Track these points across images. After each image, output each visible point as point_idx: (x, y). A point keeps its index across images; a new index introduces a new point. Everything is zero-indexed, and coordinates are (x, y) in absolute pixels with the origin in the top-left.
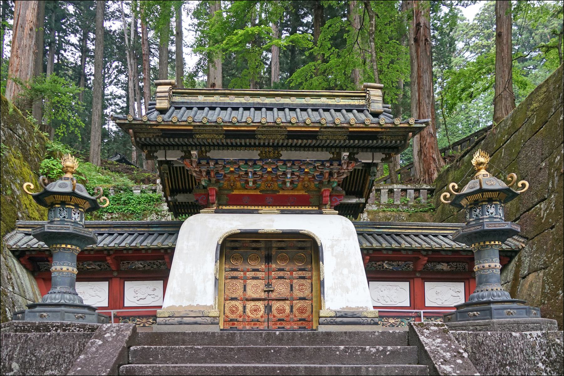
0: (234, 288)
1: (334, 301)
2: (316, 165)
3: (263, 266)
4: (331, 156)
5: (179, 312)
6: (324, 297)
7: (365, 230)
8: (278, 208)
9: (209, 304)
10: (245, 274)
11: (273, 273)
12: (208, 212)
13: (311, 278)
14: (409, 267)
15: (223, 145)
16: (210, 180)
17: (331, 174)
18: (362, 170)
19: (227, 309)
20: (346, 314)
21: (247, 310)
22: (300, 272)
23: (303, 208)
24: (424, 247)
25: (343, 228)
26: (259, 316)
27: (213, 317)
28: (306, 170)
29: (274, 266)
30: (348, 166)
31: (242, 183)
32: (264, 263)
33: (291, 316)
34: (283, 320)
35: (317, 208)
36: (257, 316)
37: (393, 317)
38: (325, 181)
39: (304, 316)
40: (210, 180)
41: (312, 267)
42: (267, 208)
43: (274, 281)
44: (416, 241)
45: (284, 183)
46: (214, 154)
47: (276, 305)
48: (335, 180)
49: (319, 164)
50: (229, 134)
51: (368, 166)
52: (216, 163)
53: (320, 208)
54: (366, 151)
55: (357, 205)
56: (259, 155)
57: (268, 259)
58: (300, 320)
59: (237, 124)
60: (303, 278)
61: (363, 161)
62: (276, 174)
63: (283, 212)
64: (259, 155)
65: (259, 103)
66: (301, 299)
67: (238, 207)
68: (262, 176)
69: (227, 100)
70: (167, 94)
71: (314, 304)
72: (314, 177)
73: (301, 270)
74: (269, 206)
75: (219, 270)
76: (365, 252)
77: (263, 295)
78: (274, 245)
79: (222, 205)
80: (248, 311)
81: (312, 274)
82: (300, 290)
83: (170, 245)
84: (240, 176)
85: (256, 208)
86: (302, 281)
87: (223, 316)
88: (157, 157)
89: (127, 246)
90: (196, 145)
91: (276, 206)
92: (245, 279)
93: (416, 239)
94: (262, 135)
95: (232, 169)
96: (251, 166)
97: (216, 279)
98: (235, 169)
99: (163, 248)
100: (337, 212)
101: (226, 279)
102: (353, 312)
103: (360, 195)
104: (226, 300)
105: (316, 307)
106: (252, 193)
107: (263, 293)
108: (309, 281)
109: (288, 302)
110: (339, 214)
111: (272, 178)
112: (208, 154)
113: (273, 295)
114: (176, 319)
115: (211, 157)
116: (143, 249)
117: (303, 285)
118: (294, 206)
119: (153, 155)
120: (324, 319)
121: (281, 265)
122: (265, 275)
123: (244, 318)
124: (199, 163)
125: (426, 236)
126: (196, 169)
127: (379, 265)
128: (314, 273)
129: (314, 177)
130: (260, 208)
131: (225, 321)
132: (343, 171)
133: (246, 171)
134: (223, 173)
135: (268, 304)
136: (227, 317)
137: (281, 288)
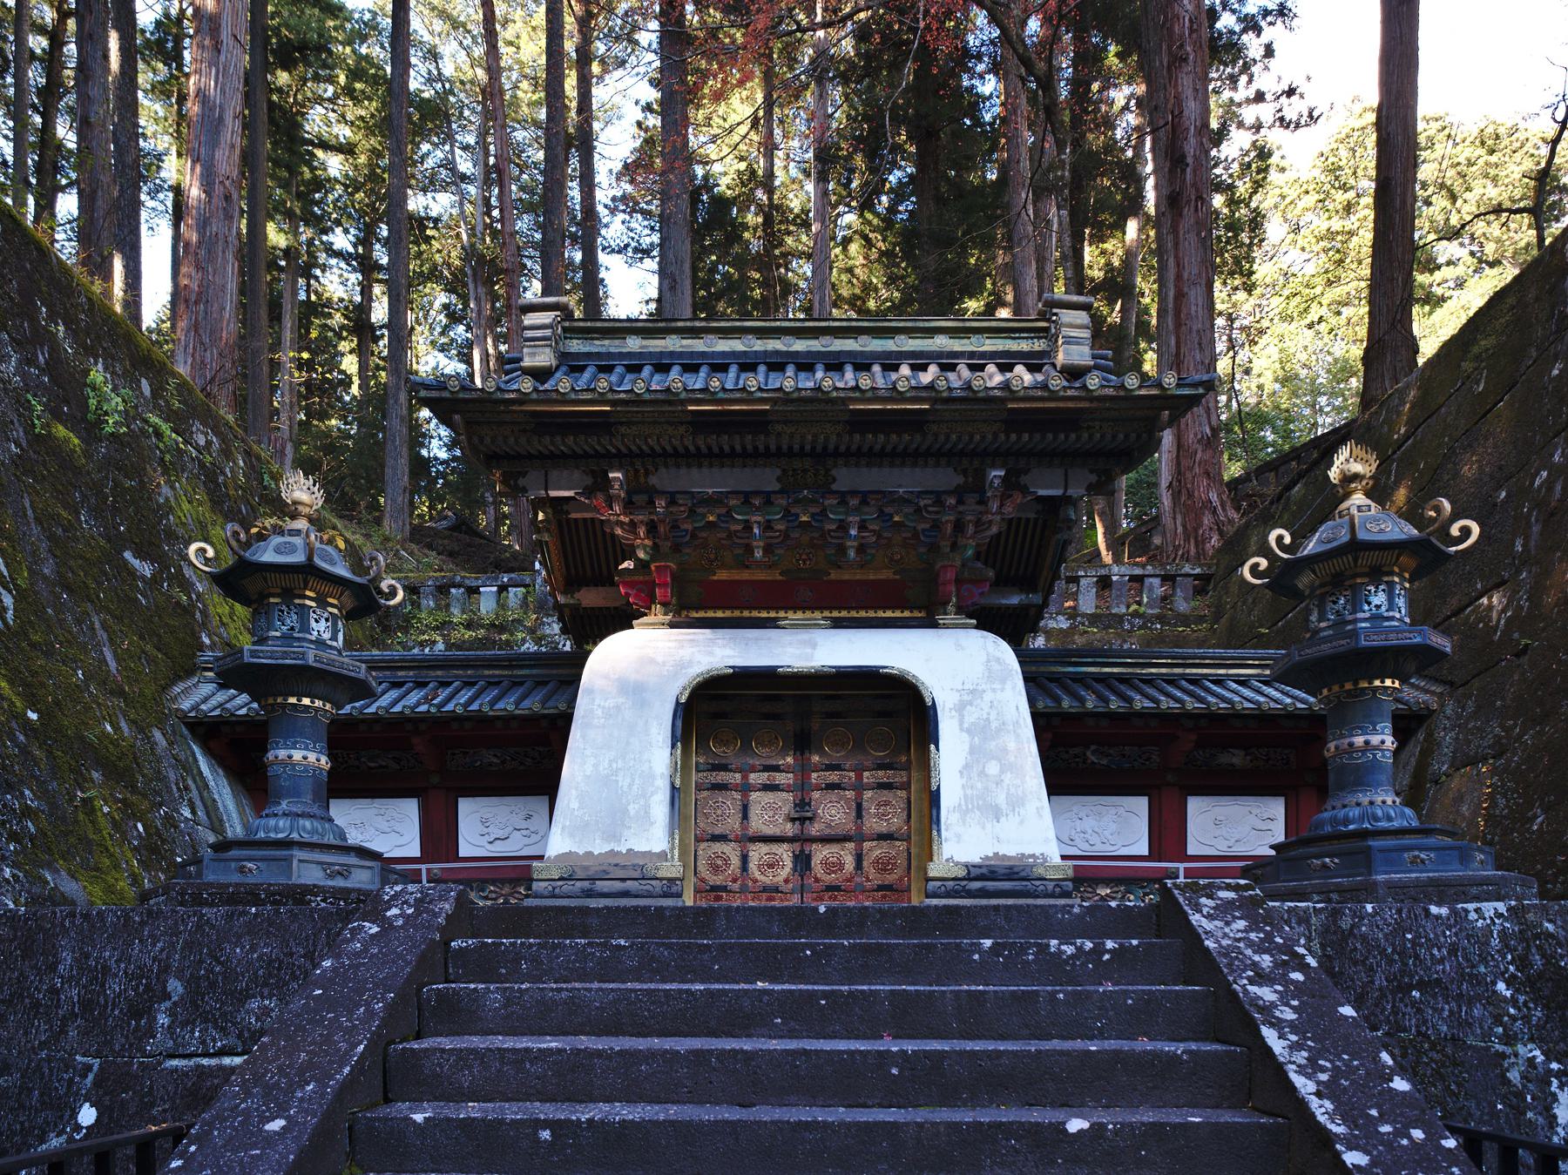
1: (963, 842)
2: (922, 503)
3: (790, 760)
4: (960, 480)
5: (586, 868)
6: (939, 831)
7: (1042, 669)
8: (827, 614)
9: (657, 850)
10: (745, 777)
11: (814, 775)
13: (906, 786)
14: (1148, 759)
15: (687, 454)
17: (959, 527)
18: (1036, 520)
19: (702, 863)
20: (993, 872)
22: (881, 773)
23: (889, 614)
24: (1189, 707)
25: (988, 661)
26: (780, 879)
27: (669, 880)
29: (816, 758)
30: (1002, 505)
33: (858, 879)
34: (837, 888)
37: (1107, 882)
38: (945, 545)
39: (890, 878)
40: (655, 547)
41: (909, 761)
42: (799, 615)
43: (816, 795)
44: (1168, 695)
45: (842, 550)
47: (820, 853)
50: (702, 423)
51: (1053, 506)
52: (672, 502)
55: (1023, 609)
57: (802, 744)
58: (880, 888)
59: (721, 395)
61: (1042, 492)
63: (838, 624)
64: (779, 479)
65: (777, 353)
66: (882, 837)
67: (728, 614)
69: (698, 345)
70: (548, 332)
73: (880, 767)
74: (804, 609)
75: (682, 768)
76: (1042, 722)
77: (790, 829)
79: (689, 608)
80: (752, 866)
81: (909, 778)
82: (880, 816)
83: (562, 706)
85: (773, 614)
86: (886, 795)
87: (693, 879)
90: (619, 455)
91: (821, 609)
92: (746, 789)
93: (1170, 689)
94: (785, 423)
96: (758, 509)
97: (673, 787)
98: (719, 516)
99: (545, 716)
101: (699, 788)
102: (1011, 868)
103: (1028, 584)
104: (698, 840)
105: (919, 855)
106: (761, 576)
107: (789, 825)
108: (903, 794)
109: (851, 845)
110: (976, 627)
111: (812, 539)
112: (654, 480)
113: (815, 829)
114: (579, 884)
115: (658, 487)
116: (498, 718)
117: (887, 803)
118: (866, 608)
120: (939, 883)
121: (836, 756)
122: (796, 779)
123: (744, 886)
125: (1194, 681)
127: (1076, 756)
129: (916, 536)
130: (782, 614)
131: (697, 891)
133: (747, 521)
134: (688, 527)
135: (802, 851)
136: (703, 880)
137: (832, 812)
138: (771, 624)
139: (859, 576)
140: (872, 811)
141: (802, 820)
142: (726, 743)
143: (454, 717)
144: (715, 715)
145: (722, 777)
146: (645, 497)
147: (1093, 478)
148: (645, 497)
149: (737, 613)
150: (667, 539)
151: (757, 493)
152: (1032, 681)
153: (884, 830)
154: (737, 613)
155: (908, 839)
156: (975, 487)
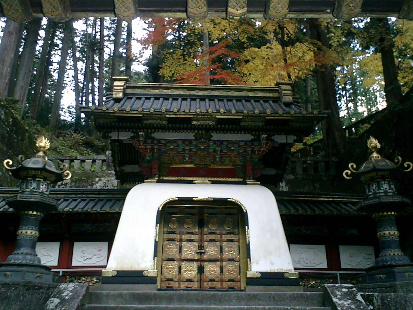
0: (171, 250)
3: (197, 230)
4: (253, 137)
8: (210, 179)
11: (205, 236)
12: (151, 182)
16: (153, 155)
17: (253, 152)
21: (182, 271)
22: (229, 235)
28: (232, 148)
31: (179, 158)
32: (197, 227)
35: (241, 180)
36: (191, 276)
38: (248, 157)
40: (153, 155)
43: (206, 243)
45: (215, 158)
46: (158, 135)
48: (256, 158)
49: (243, 144)
53: (245, 179)
54: (281, 134)
56: (194, 136)
57: (201, 224)
60: (232, 241)
62: (208, 151)
63: (214, 183)
64: (194, 136)
68: (196, 153)
71: (242, 266)
72: (239, 153)
77: (196, 257)
78: (206, 211)
79: (163, 176)
82: (229, 252)
83: (117, 210)
84: (178, 152)
85: (191, 179)
88: (111, 137)
89: (80, 211)
91: (208, 177)
92: (181, 240)
95: (172, 147)
100: (259, 183)
107: (196, 255)
108: (237, 244)
109: (218, 263)
110: (260, 185)
112: (153, 135)
113: (205, 257)
117: (232, 247)
118: (223, 177)
119: (108, 135)
121: (212, 228)
124: (145, 142)
126: (143, 147)
128: (240, 236)
129: (239, 153)
130: (194, 179)
132: (263, 149)
135: (201, 265)
137: (211, 250)
138: (191, 182)
139: (220, 166)
140: (226, 250)
141: (201, 253)
142: (174, 223)
143: (78, 213)
144: (170, 215)
145: (172, 236)
146: (150, 140)
147: (295, 138)
148: (150, 140)
149: (179, 178)
150: (157, 153)
151: (187, 140)
152: (279, 202)
153: (231, 258)
154: (179, 178)
155: (239, 261)
156: (258, 139)
